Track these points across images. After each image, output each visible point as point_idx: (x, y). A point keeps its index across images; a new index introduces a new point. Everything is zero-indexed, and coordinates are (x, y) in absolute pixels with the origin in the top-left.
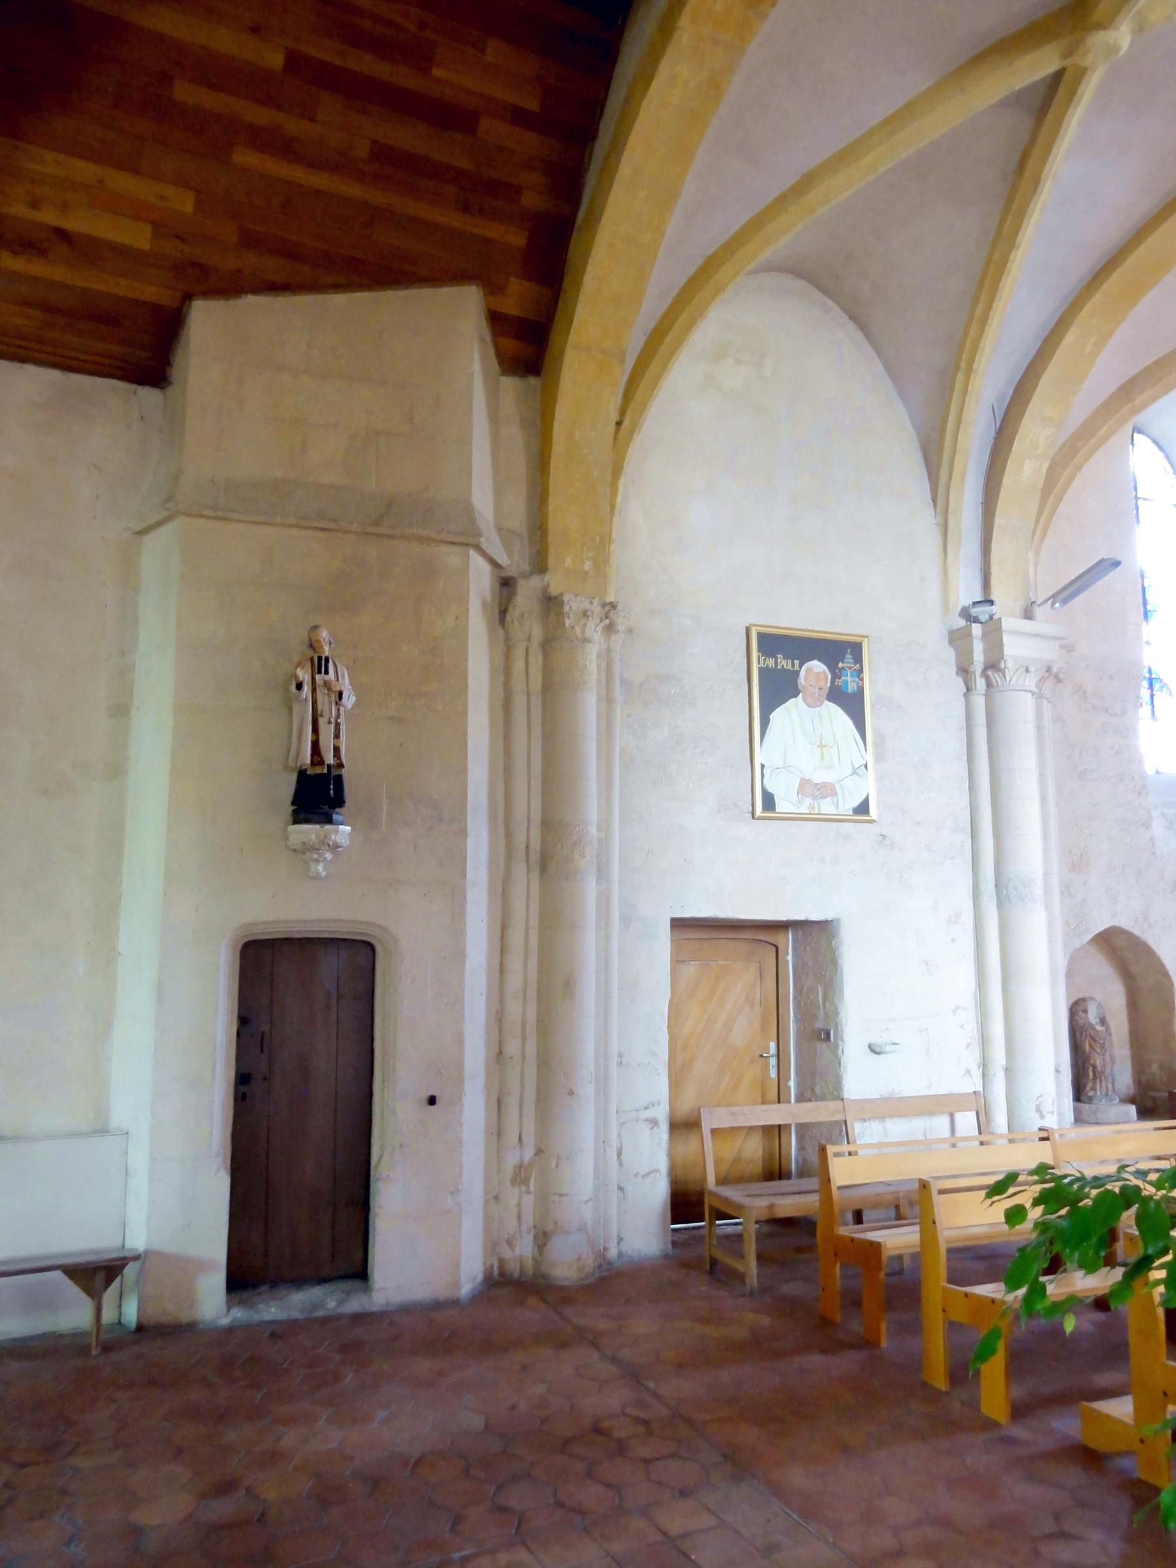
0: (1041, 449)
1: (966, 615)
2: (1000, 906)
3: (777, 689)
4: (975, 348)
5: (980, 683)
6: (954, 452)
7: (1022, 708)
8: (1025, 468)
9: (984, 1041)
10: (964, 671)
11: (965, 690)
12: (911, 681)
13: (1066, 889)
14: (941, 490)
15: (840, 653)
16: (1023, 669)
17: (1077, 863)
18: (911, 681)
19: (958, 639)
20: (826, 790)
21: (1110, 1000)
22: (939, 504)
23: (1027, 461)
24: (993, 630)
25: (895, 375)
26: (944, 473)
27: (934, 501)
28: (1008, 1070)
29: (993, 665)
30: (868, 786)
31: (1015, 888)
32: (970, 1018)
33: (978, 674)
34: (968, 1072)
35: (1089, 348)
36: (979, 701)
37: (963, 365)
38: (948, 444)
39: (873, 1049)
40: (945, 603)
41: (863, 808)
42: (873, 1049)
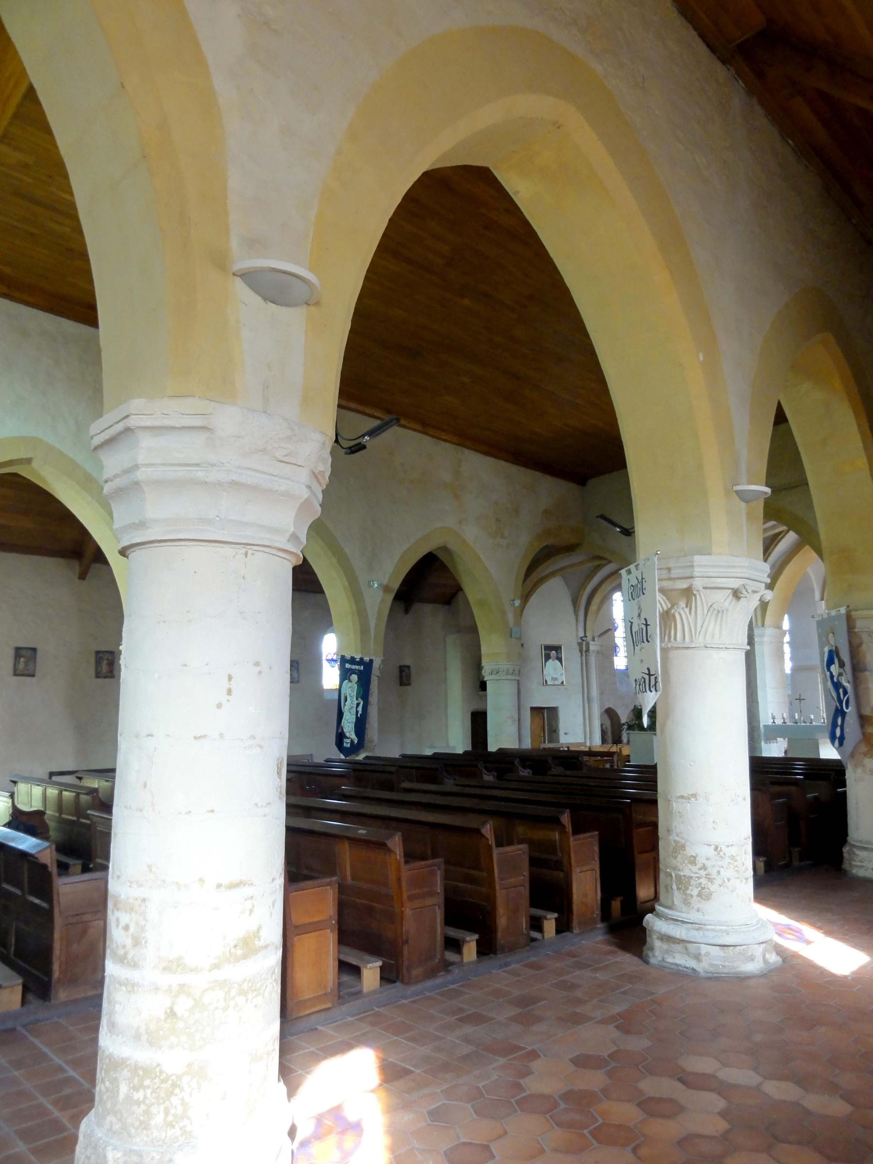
3: (548, 657)
7: (593, 659)
8: (593, 607)
9: (585, 732)
10: (581, 651)
12: (570, 653)
13: (600, 700)
15: (557, 649)
17: (602, 693)
18: (570, 653)
19: (580, 645)
20: (556, 679)
21: (608, 723)
24: (588, 645)
25: (567, 584)
29: (587, 650)
30: (564, 679)
32: (582, 727)
36: (584, 658)
39: (566, 734)
40: (577, 636)
41: (562, 683)
42: (566, 734)
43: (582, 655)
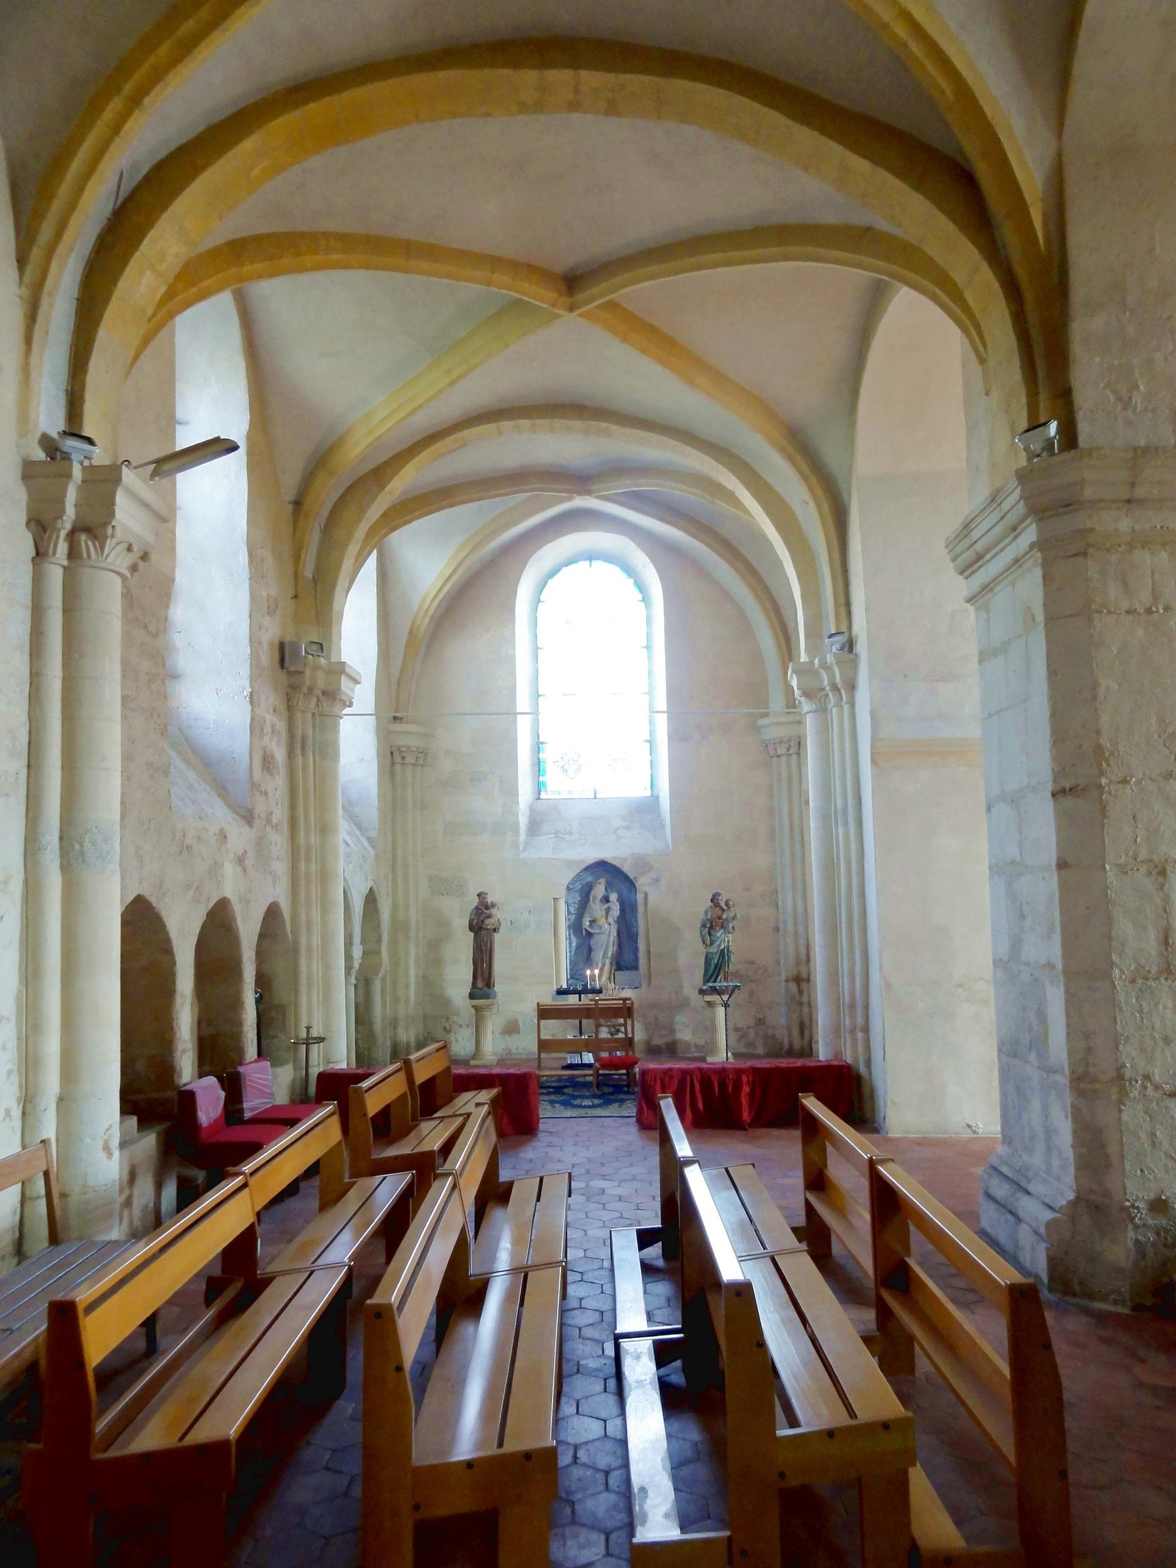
0: (165, 265)
1: (50, 446)
2: (66, 867)
4: (157, 76)
5: (63, 548)
6: (72, 206)
10: (40, 526)
11: (34, 554)
14: (36, 253)
16: (125, 545)
22: (29, 269)
23: (148, 273)
24: (103, 482)
26: (47, 229)
27: (22, 261)
28: (62, 1100)
29: (93, 526)
31: (94, 843)
33: (63, 534)
34: (8, 1112)
35: (256, 172)
36: (55, 575)
37: (127, 89)
38: (64, 190)
43: (40, 554)
